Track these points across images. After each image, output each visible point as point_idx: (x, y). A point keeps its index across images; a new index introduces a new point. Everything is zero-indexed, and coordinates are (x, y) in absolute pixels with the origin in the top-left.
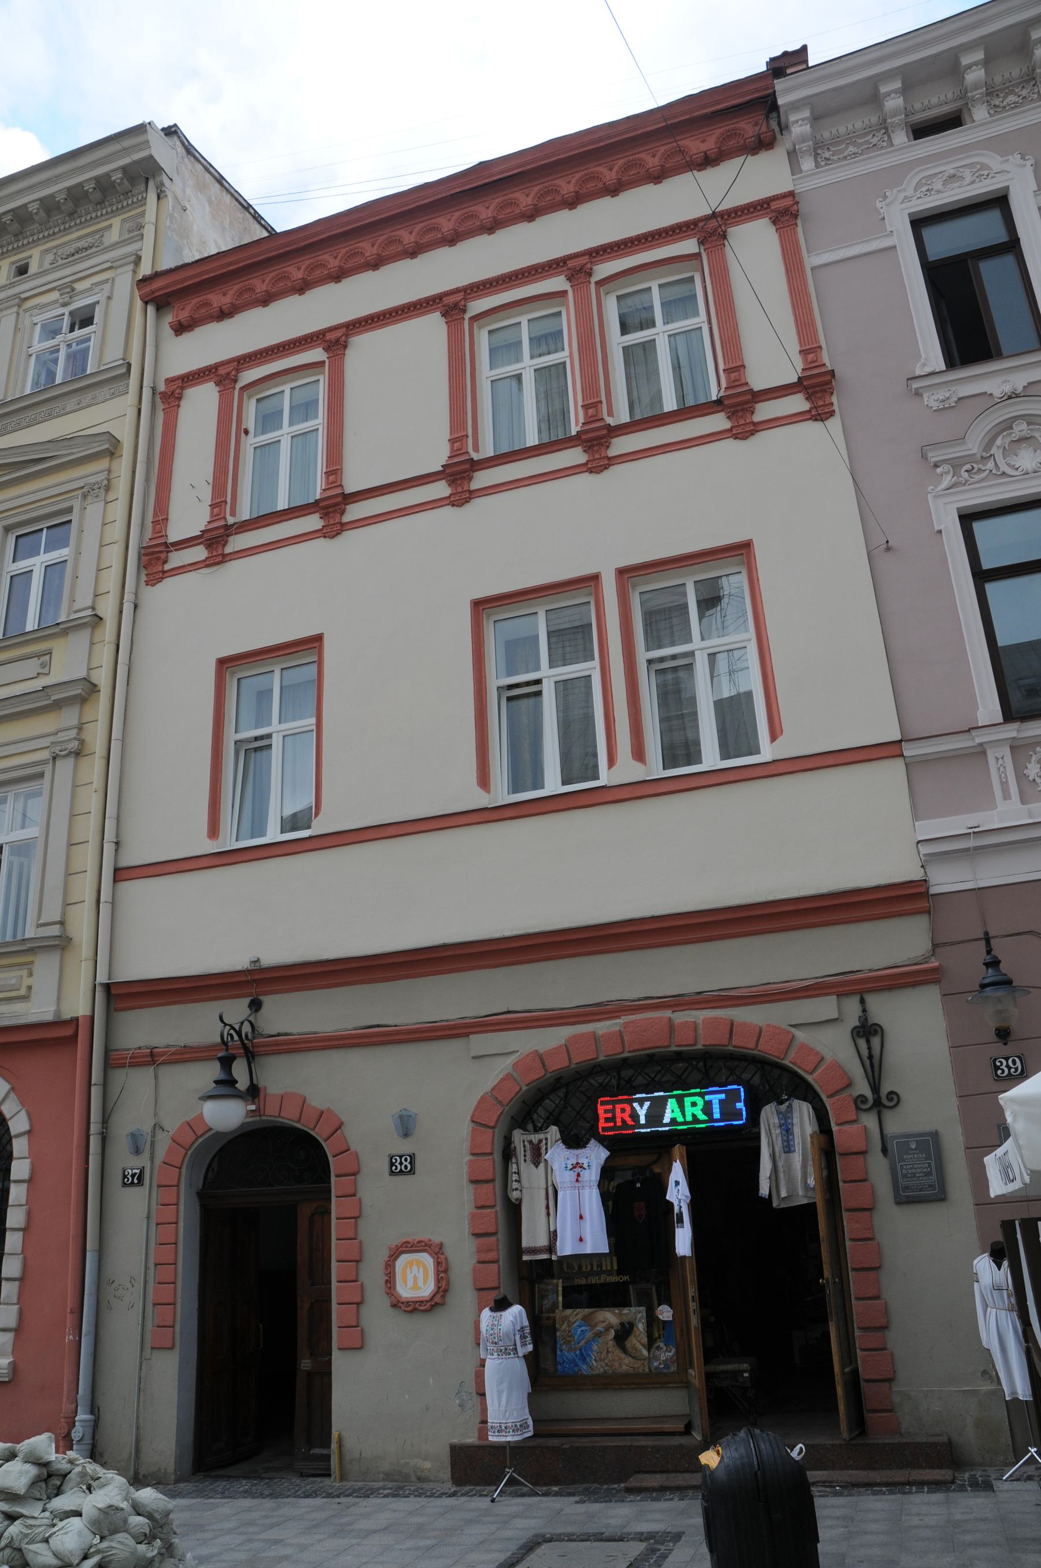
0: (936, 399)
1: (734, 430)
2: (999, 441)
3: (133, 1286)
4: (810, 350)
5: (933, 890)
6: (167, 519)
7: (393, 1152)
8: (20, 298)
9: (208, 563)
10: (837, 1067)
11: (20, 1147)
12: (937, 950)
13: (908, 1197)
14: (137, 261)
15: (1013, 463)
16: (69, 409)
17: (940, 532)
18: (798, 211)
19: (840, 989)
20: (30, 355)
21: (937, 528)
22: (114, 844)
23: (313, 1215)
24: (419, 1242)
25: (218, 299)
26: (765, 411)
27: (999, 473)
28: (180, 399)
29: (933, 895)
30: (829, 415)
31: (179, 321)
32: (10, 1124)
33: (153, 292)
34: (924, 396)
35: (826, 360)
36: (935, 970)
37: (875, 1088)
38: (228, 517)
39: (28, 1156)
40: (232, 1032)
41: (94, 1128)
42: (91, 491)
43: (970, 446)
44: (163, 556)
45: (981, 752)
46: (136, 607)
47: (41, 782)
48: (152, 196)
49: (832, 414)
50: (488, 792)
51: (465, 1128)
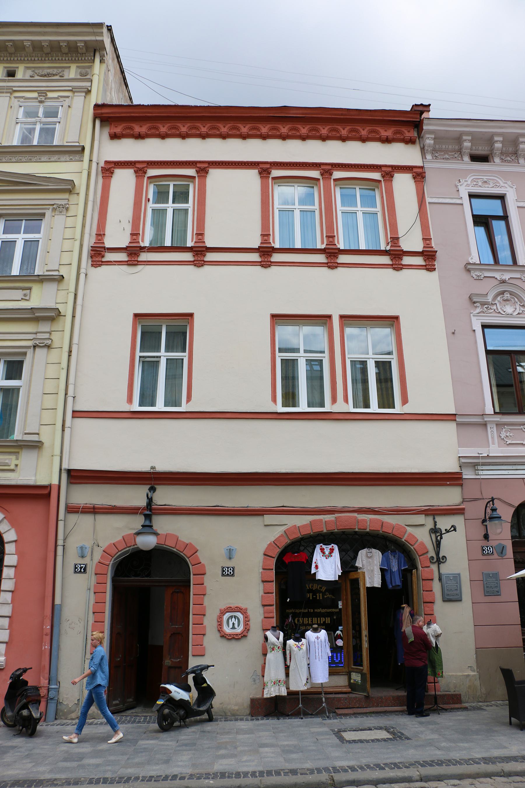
0: (476, 274)
1: (394, 265)
2: (499, 298)
3: (80, 623)
4: (427, 239)
5: (464, 477)
6: (104, 235)
7: (224, 566)
8: (12, 89)
9: (129, 263)
10: (422, 544)
11: (9, 548)
12: (464, 502)
13: (448, 598)
15: (503, 309)
16: (43, 160)
17: (474, 331)
18: (425, 176)
19: (426, 512)
21: (474, 329)
22: (73, 398)
23: (173, 592)
24: (236, 607)
25: (137, 129)
26: (407, 260)
27: (498, 312)
29: (464, 479)
30: (433, 270)
31: (115, 133)
33: (102, 114)
34: (471, 272)
35: (433, 245)
36: (463, 509)
37: (438, 554)
38: (140, 242)
39: (15, 553)
41: (60, 542)
42: (57, 208)
43: (489, 298)
45: (485, 425)
47: (24, 357)
48: (97, 60)
49: (435, 269)
50: (276, 405)
51: (260, 557)
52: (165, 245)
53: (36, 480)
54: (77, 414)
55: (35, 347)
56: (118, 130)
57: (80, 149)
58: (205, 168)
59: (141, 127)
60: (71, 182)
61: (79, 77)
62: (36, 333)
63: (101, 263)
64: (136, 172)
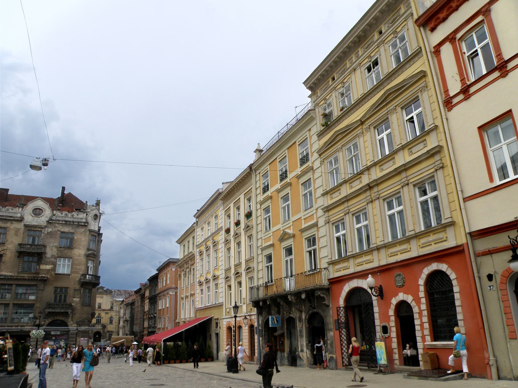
6: (448, 90)
11: (455, 283)
14: (412, 14)
20: (391, 56)
25: (441, 16)
28: (440, 51)
32: (450, 277)
33: (420, 23)
38: (467, 82)
40: (514, 241)
44: (450, 101)
46: (447, 119)
52: (484, 74)
53: (457, 243)
54: (465, 200)
55: (436, 170)
56: (432, 25)
57: (420, 50)
58: (487, 9)
59: (443, 13)
60: (422, 71)
61: (406, 9)
62: (434, 163)
63: (452, 107)
64: (450, 42)
